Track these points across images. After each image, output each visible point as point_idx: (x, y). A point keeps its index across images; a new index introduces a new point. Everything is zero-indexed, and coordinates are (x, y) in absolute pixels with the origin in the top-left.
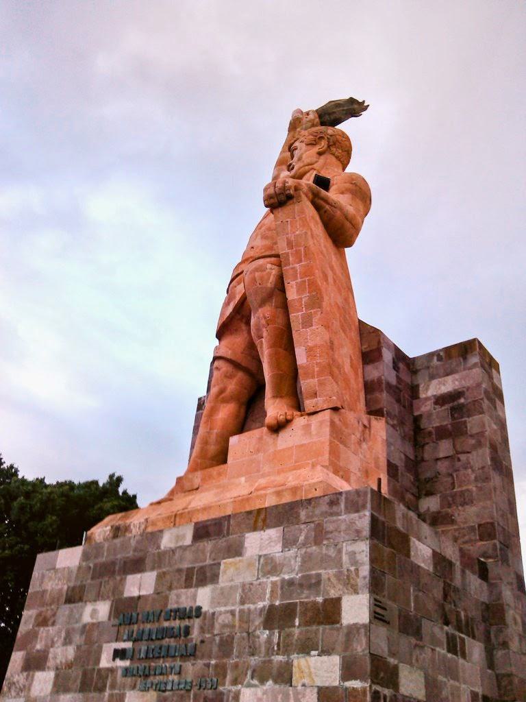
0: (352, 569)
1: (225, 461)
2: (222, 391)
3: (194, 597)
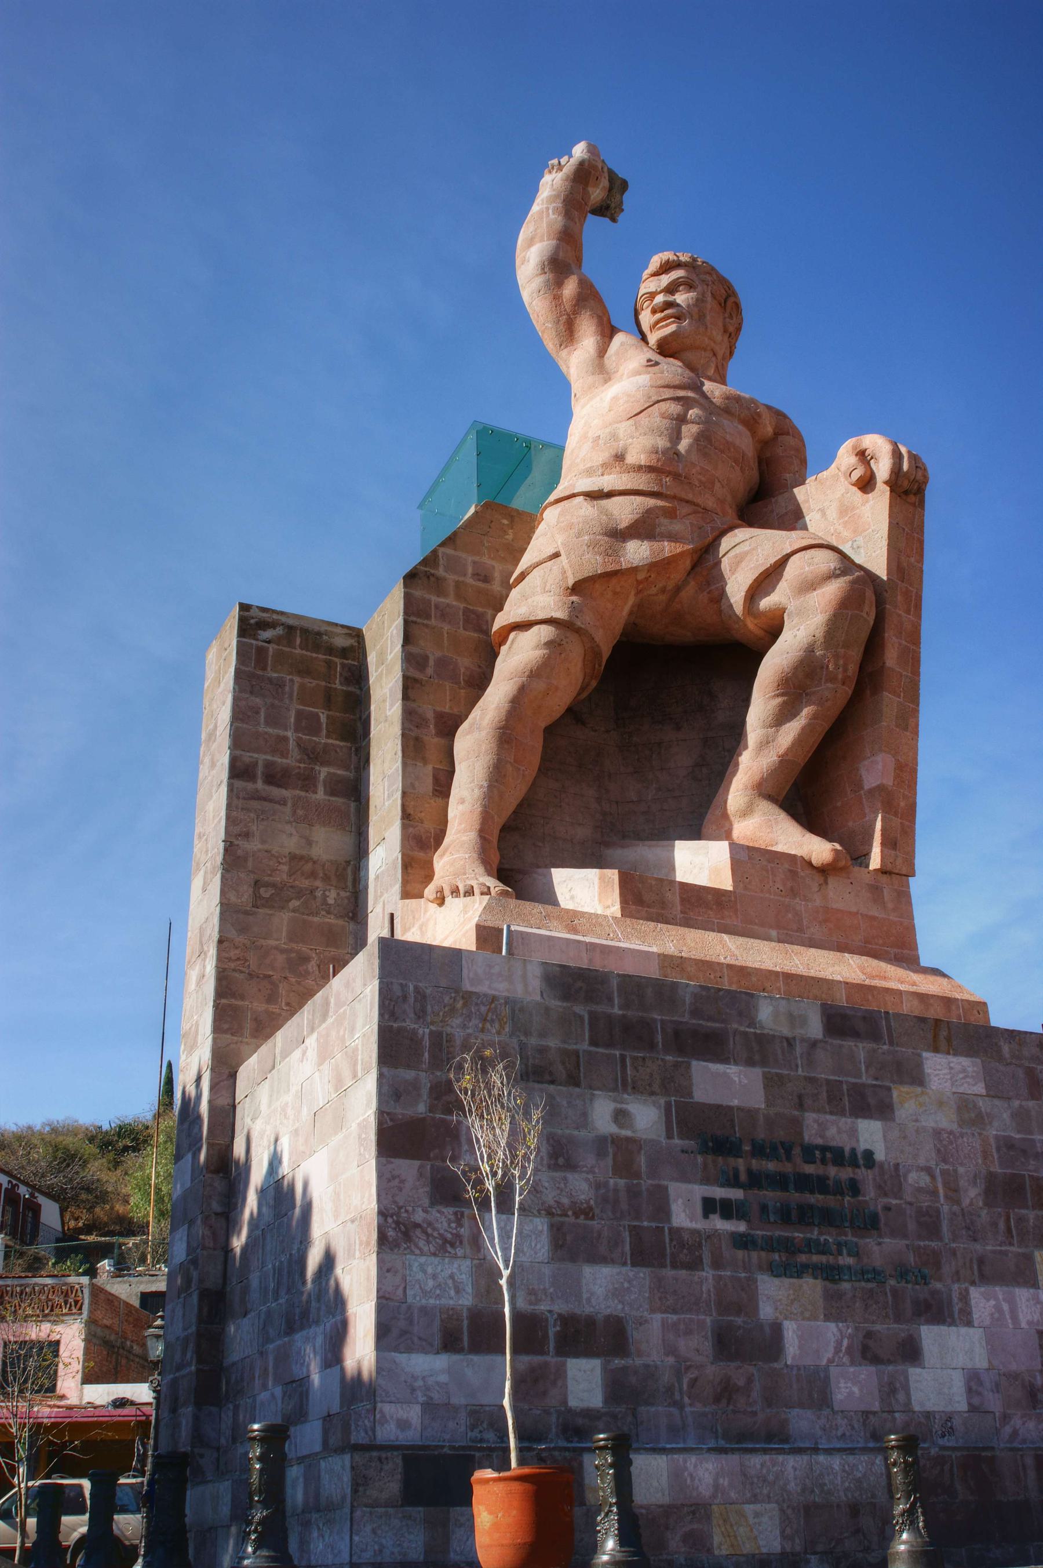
3: (853, 1132)
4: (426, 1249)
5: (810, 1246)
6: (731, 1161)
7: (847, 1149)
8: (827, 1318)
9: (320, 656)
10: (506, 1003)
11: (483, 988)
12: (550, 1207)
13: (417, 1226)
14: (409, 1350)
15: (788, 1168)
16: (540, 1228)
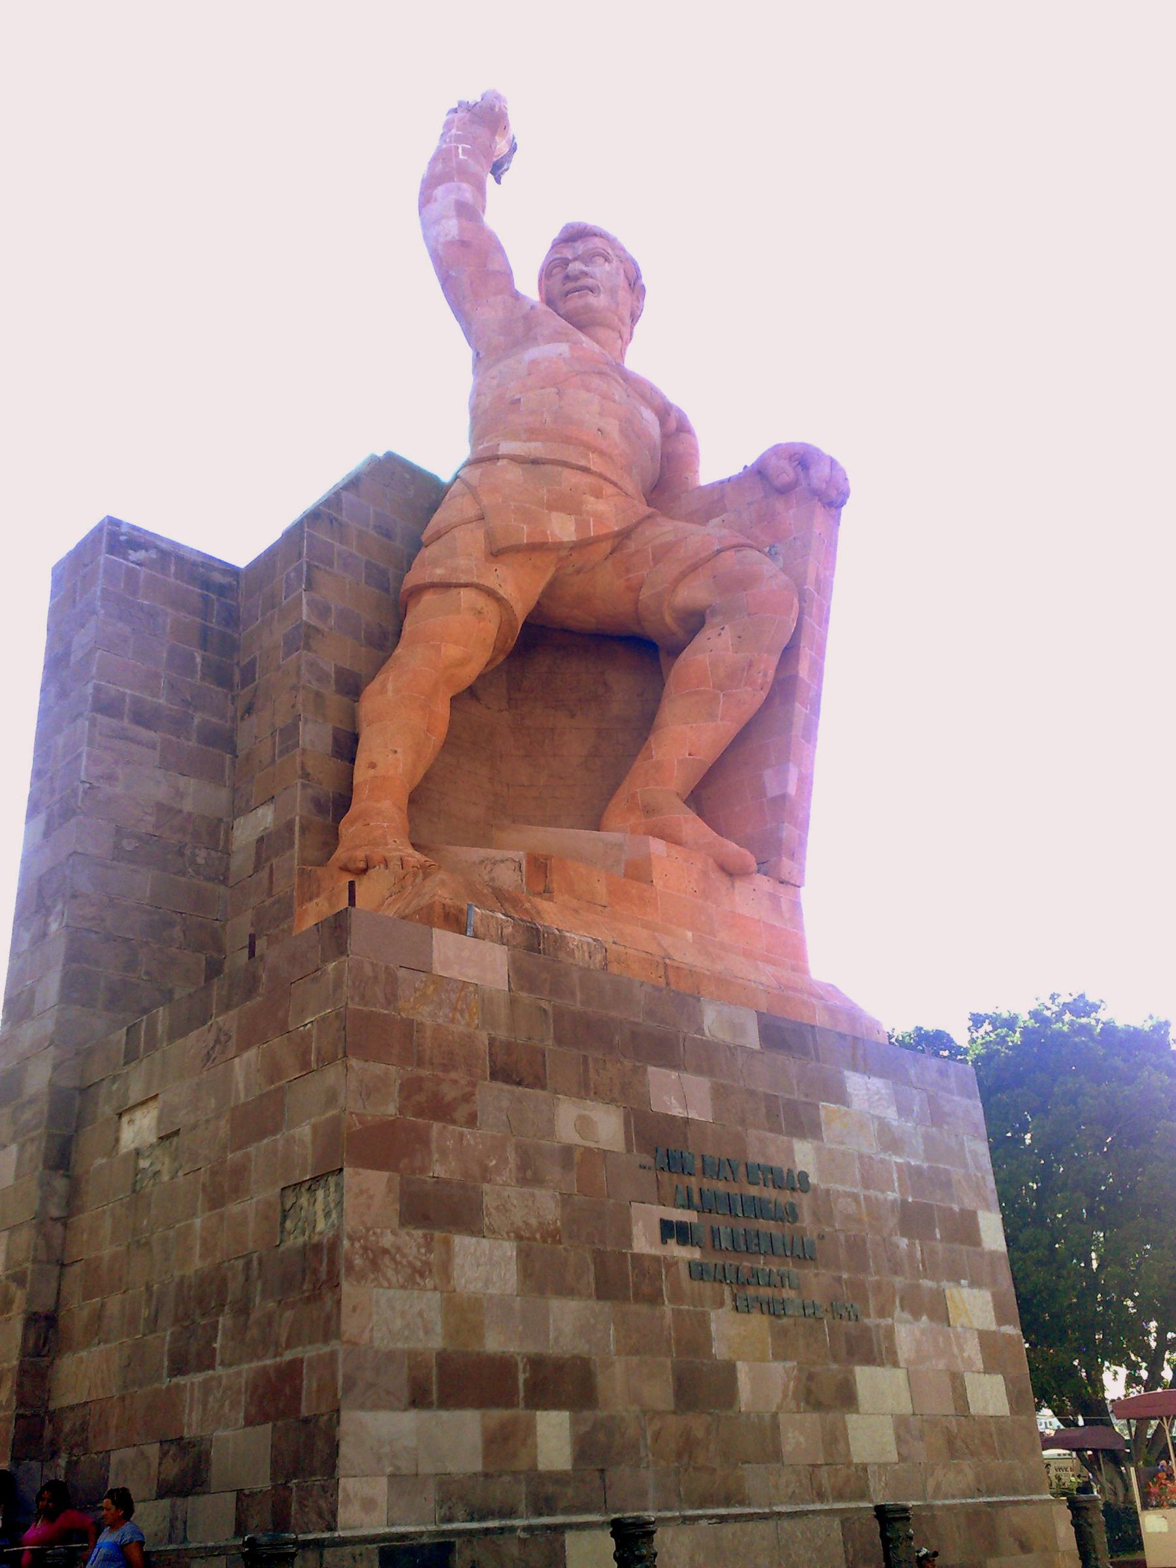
0: (979, 1175)
2: (462, 663)
3: (790, 1153)
4: (394, 1280)
5: (754, 1277)
6: (686, 1178)
7: (785, 1170)
8: (777, 1357)
9: (196, 590)
10: (476, 992)
11: (453, 973)
12: (519, 1228)
13: (385, 1251)
14: (375, 1407)
15: (734, 1189)
16: (509, 1254)
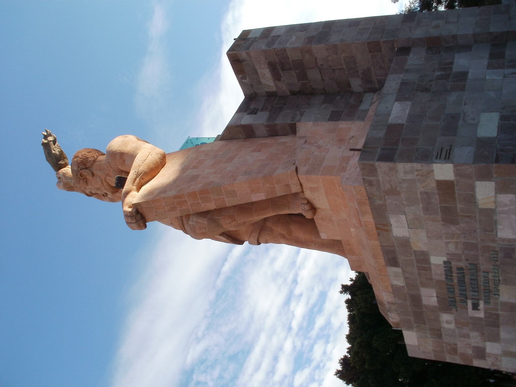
0: (416, 173)
1: (340, 242)
